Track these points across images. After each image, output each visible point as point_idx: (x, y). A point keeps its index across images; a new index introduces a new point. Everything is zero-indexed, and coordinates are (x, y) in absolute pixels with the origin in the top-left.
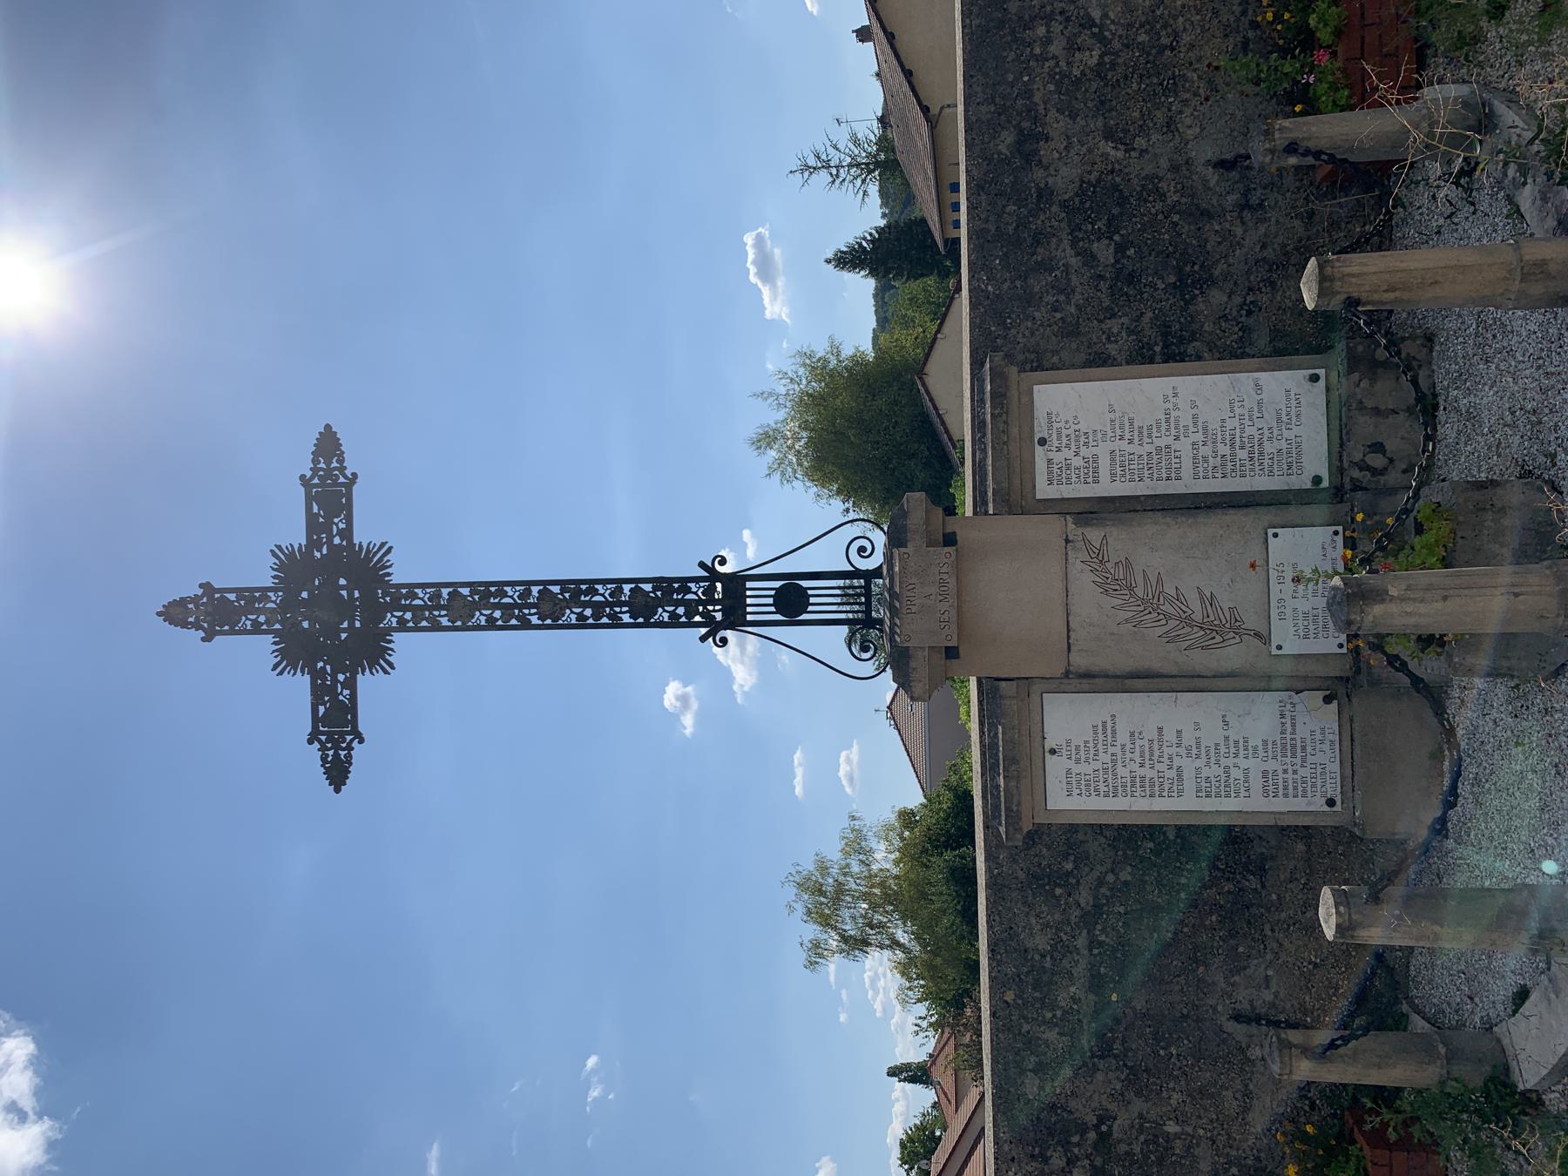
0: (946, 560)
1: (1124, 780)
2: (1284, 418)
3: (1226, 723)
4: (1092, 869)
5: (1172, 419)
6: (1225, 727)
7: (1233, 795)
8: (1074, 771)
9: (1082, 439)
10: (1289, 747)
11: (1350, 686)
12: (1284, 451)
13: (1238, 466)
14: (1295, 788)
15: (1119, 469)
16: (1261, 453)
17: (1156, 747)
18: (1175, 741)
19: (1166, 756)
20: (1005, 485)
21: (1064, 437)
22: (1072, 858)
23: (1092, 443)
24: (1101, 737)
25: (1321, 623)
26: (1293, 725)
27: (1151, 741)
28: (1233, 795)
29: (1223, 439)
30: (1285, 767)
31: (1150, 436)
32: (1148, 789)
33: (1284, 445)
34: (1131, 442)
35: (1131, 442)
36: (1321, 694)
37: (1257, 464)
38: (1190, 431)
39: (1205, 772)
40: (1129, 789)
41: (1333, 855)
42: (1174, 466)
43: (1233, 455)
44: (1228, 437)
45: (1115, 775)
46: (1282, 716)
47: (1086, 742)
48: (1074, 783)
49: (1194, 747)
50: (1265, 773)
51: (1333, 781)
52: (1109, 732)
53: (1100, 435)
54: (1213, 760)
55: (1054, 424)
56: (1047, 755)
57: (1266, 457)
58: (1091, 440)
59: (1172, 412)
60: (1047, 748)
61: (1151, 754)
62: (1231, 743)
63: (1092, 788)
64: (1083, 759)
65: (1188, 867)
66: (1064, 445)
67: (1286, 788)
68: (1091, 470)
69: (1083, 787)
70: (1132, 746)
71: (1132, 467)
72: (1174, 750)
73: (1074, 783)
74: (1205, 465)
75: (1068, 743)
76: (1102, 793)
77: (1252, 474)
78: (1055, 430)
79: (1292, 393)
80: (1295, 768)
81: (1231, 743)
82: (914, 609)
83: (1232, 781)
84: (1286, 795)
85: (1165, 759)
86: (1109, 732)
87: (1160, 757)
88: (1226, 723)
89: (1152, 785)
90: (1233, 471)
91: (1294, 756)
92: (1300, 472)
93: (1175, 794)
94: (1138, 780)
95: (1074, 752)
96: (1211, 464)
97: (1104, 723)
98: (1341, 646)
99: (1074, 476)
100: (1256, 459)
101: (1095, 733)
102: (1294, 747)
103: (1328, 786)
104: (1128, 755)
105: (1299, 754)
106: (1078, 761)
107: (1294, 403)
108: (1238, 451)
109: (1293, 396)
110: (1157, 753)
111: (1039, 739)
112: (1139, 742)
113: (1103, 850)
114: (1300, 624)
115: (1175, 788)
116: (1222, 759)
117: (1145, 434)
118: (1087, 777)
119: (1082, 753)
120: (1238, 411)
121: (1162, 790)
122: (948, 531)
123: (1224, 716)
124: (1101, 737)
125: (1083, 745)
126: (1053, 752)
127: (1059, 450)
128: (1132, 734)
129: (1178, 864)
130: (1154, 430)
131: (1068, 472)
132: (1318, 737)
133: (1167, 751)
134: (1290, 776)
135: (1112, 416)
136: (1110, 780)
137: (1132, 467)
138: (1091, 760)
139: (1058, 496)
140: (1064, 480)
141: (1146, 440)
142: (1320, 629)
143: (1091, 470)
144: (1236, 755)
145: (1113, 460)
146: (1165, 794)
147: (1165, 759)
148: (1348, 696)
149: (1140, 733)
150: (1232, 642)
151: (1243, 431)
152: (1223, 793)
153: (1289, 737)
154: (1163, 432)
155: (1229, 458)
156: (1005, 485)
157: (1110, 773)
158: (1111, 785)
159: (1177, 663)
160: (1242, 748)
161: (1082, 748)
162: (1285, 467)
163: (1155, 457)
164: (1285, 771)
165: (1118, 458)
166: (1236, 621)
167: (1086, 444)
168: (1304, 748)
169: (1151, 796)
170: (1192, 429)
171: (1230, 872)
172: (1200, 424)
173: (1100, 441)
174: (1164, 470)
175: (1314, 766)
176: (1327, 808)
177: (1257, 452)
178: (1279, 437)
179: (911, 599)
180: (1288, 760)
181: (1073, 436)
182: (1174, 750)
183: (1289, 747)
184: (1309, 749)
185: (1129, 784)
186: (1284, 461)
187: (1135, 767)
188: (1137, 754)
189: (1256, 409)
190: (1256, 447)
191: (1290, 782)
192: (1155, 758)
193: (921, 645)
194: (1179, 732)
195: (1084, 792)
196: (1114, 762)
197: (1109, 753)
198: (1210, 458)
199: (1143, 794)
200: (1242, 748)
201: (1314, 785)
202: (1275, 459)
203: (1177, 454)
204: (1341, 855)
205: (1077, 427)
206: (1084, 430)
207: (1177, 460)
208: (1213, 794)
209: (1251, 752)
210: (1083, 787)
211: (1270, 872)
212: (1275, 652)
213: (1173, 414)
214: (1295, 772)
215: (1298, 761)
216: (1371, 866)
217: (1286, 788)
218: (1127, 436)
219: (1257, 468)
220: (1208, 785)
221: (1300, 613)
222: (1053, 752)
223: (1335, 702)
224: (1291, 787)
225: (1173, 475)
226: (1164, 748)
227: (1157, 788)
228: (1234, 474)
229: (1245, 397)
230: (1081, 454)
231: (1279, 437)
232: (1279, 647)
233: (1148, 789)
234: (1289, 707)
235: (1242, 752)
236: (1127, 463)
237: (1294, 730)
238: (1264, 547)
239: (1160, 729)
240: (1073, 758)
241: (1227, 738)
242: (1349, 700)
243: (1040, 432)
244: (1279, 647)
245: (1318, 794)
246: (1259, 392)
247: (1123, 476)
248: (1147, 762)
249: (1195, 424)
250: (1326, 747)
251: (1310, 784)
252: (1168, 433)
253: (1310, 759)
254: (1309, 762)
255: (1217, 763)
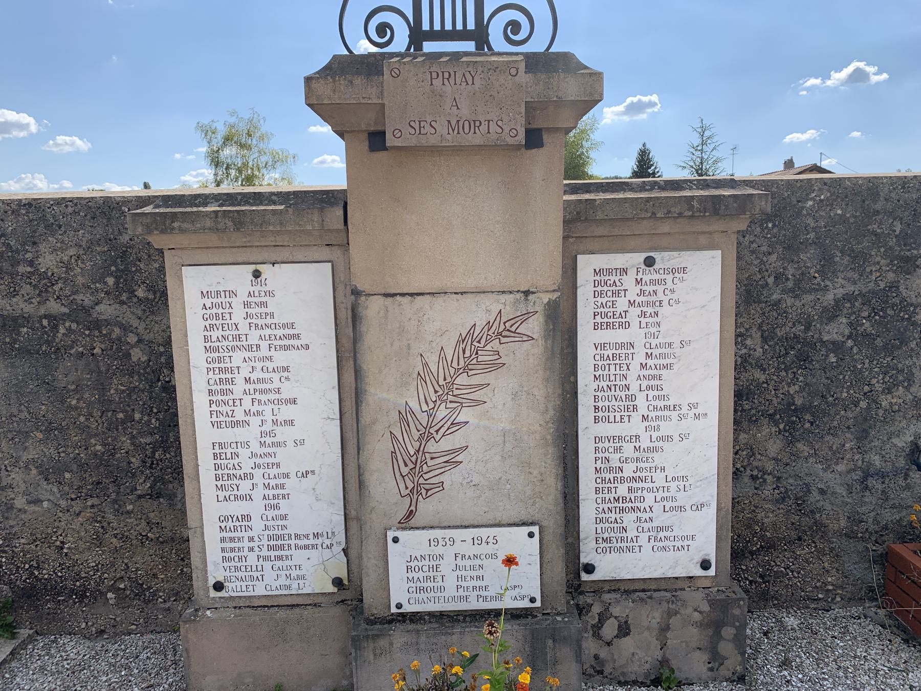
0: (506, 130)
1: (227, 360)
2: (662, 535)
3: (305, 474)
4: (140, 318)
5: (667, 413)
6: (300, 474)
7: (219, 483)
8: (234, 300)
9: (650, 310)
10: (280, 542)
11: (354, 603)
12: (624, 535)
13: (609, 485)
14: (232, 550)
15: (610, 353)
16: (622, 510)
17: (272, 396)
18: (280, 418)
19: (260, 408)
20: (600, 215)
21: (654, 288)
22: (151, 296)
23: (644, 320)
24: (280, 332)
25: (425, 585)
26: (306, 547)
27: (278, 391)
28: (219, 483)
29: (641, 470)
30: (256, 539)
31: (649, 388)
32: (219, 387)
33: (631, 533)
34: (643, 366)
35: (643, 366)
36: (343, 574)
37: (610, 505)
38: (652, 433)
39: (244, 453)
40: (217, 365)
41: (181, 563)
42: (612, 415)
43: (622, 480)
44: (643, 474)
45: (233, 349)
46: (316, 536)
47: (272, 315)
48: (219, 300)
49: (275, 440)
50: (247, 518)
51: (244, 588)
52: (286, 342)
53: (653, 330)
54: (259, 461)
55: (671, 276)
56: (253, 267)
57: (618, 516)
58: (647, 320)
59: (677, 413)
60: (260, 267)
61: (262, 392)
62: (282, 481)
63: (214, 322)
64: (250, 311)
65: (153, 420)
66: (644, 288)
67: (232, 540)
68: (611, 320)
69: (214, 311)
70: (270, 369)
71: (612, 367)
72: (268, 417)
73: (219, 300)
74: (611, 450)
75: (270, 293)
76: (208, 334)
77: (599, 501)
78: (663, 277)
79: (690, 542)
80: (256, 549)
81: (282, 481)
82: (437, 82)
83: (236, 481)
84: (223, 540)
85: (256, 407)
86: (286, 342)
87: (259, 401)
88: (305, 474)
89: (223, 392)
90: (603, 480)
91: (270, 548)
92: (600, 550)
93: (214, 419)
94: (229, 376)
95: (258, 300)
96: (612, 456)
97: (297, 337)
98: (399, 606)
99: (604, 300)
100: (616, 504)
101: (285, 326)
102: (281, 547)
103: (238, 584)
104: (259, 365)
105: (273, 554)
106: (247, 305)
107: (679, 544)
108: (626, 485)
109: (686, 543)
110: (263, 398)
111: (274, 258)
112: (276, 377)
113: (163, 331)
114: (424, 562)
115: (222, 418)
116: (261, 471)
117: (652, 383)
118: (227, 316)
119: (258, 310)
120: (673, 485)
121: (218, 403)
122: (545, 137)
123: (313, 472)
124: (280, 332)
125: (268, 310)
126: (257, 274)
127: (638, 282)
128: (286, 369)
129: (155, 410)
130: (656, 393)
131: (610, 294)
132: (294, 573)
133: (268, 409)
134: (246, 544)
135: (677, 344)
136: (225, 343)
137: (612, 367)
138: (249, 320)
139: (580, 282)
140: (599, 289)
141: (645, 383)
142: (419, 584)
143: (611, 320)
144: (267, 486)
145: (622, 345)
146: (214, 407)
147: (256, 407)
148: (342, 601)
149: (287, 379)
150: (402, 486)
151: (649, 490)
152: (220, 472)
153: (293, 542)
154: (653, 403)
155: (619, 476)
156: (600, 215)
157: (235, 343)
158: (220, 344)
159: (374, 423)
160: (276, 492)
161: (264, 310)
162: (606, 535)
163: (623, 394)
164: (251, 539)
165: (624, 351)
166: (427, 490)
167: (643, 314)
168: (279, 558)
169: (210, 391)
170: (655, 435)
171: (152, 463)
172: (661, 444)
173: (647, 330)
174: (607, 403)
175: (260, 568)
176: (211, 582)
177: (625, 505)
178: (640, 529)
179: (452, 80)
180: (265, 542)
181: (654, 298)
182: (268, 417)
183: (280, 542)
184: (279, 564)
185: (222, 365)
186: (612, 534)
187: (245, 372)
188: (262, 375)
189: (674, 504)
190: (630, 505)
191: (240, 545)
192: (258, 396)
193: (385, 94)
194: (291, 423)
195: (209, 312)
196: (250, 348)
197: (261, 342)
198: (619, 455)
199: (212, 382)
200: (276, 492)
201: (237, 569)
202: (616, 525)
203: (626, 419)
204: (182, 570)
205: (665, 303)
206: (661, 311)
207: (618, 419)
208: (219, 461)
209: (272, 502)
210: (214, 311)
211: (156, 503)
212: (391, 535)
213: (674, 414)
214: (251, 549)
215: (265, 552)
216: (172, 599)
217: (232, 540)
218: (650, 362)
219: (606, 506)
220: (229, 456)
221: (437, 562)
222: (257, 274)
223: (335, 590)
224: (233, 545)
225: (600, 414)
226: (271, 406)
227: (220, 398)
228: (599, 481)
229: (690, 493)
230: (631, 309)
231: (640, 529)
232: (396, 540)
233: (219, 387)
234: (328, 542)
235: (271, 492)
236: (617, 362)
237: (301, 548)
238: (517, 520)
239: (294, 401)
240: (250, 299)
241: (287, 476)
242: (338, 603)
243: (662, 259)
244: (396, 540)
245: (228, 574)
246: (694, 508)
247: (602, 357)
248: (252, 387)
249: (661, 439)
250: (283, 581)
251: (239, 565)
252: (651, 408)
253: (267, 565)
254: (264, 563)
255: (256, 466)
